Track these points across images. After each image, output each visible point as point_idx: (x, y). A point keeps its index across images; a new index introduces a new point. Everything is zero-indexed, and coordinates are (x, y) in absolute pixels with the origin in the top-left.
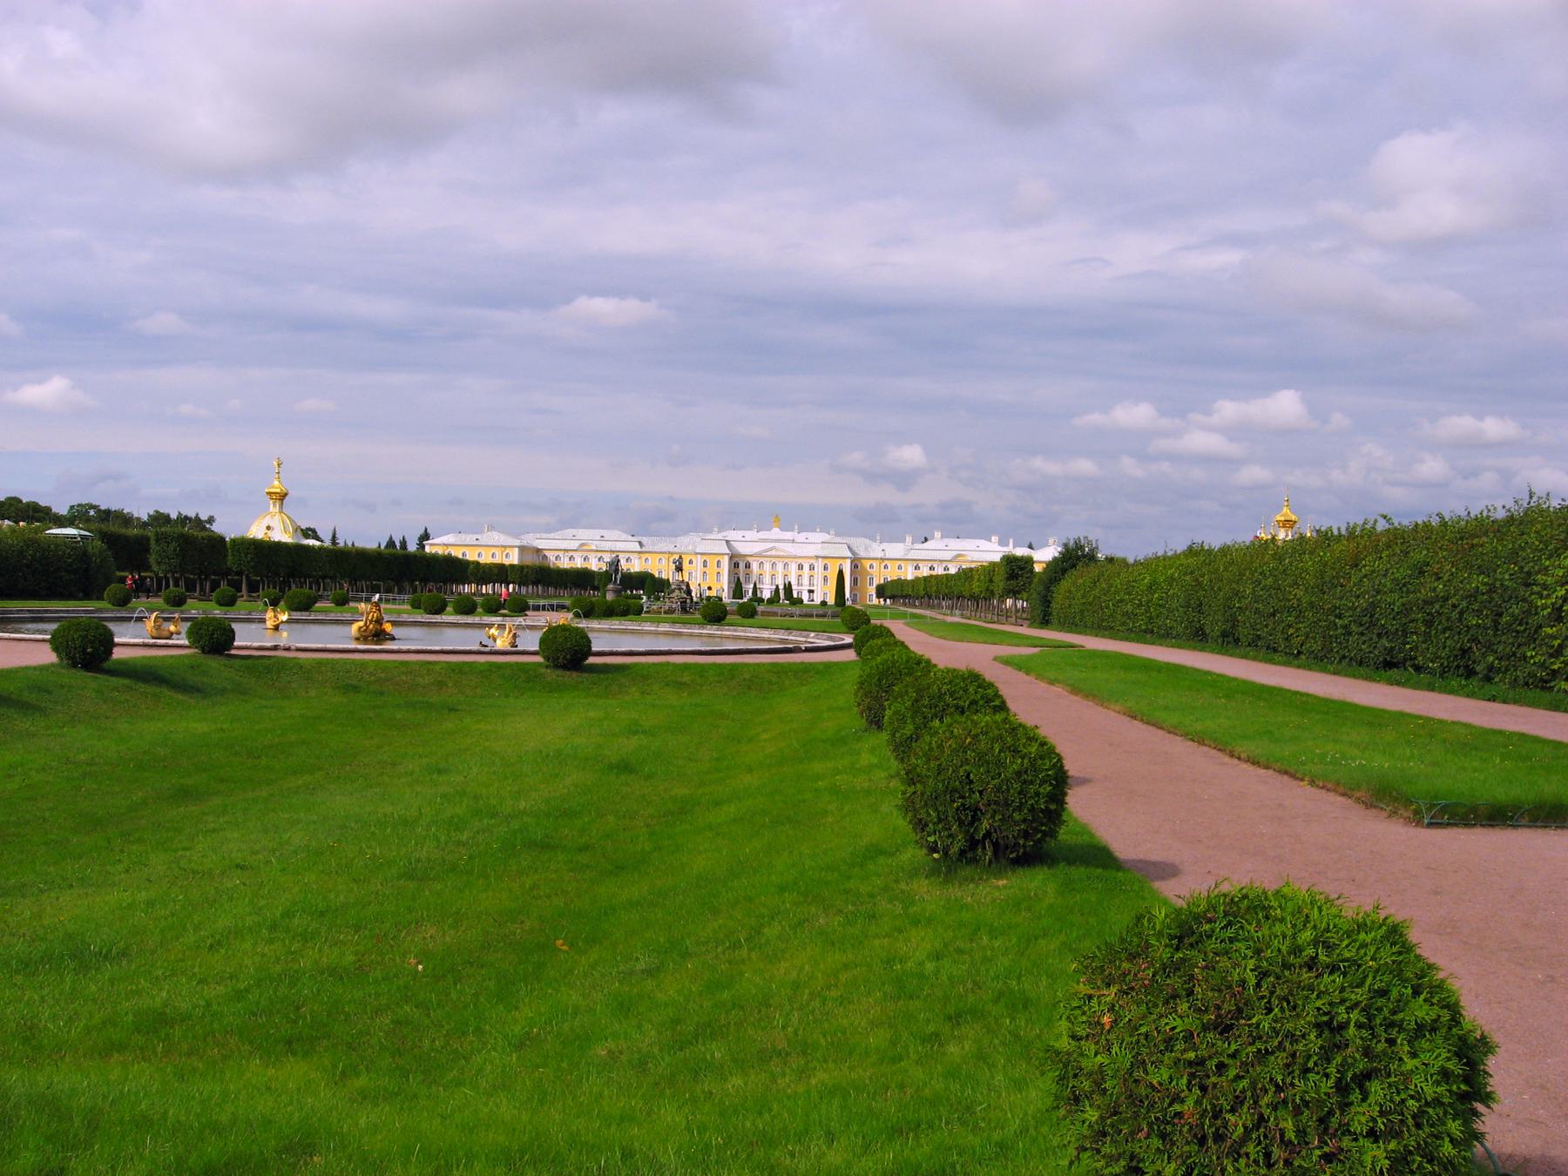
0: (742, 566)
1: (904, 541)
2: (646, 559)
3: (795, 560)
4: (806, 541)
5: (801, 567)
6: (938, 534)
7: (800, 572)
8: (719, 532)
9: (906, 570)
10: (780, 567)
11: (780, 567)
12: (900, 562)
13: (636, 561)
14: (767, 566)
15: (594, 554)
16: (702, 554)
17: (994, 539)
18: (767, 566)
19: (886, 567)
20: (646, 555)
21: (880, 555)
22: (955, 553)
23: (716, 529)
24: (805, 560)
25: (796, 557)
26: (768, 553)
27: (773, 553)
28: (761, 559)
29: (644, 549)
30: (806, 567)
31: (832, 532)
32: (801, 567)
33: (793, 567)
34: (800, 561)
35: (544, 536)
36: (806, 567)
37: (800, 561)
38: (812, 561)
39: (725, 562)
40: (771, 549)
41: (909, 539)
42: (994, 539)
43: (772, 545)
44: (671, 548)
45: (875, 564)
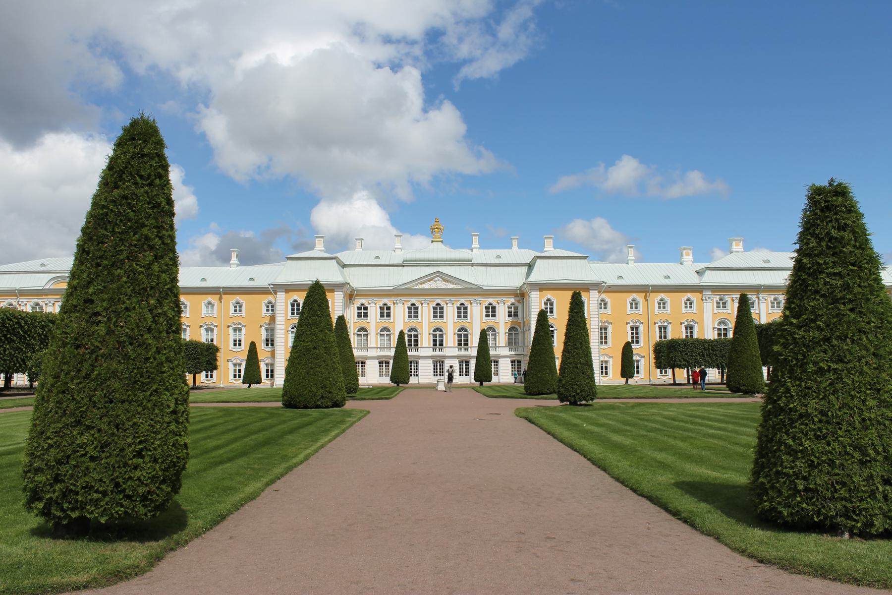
0: (374, 311)
3: (479, 298)
4: (497, 261)
9: (701, 310)
10: (450, 312)
11: (450, 312)
12: (689, 295)
14: (426, 311)
18: (426, 311)
19: (662, 304)
24: (499, 299)
26: (426, 286)
27: (440, 284)
30: (502, 312)
32: (491, 311)
40: (430, 278)
45: (639, 297)
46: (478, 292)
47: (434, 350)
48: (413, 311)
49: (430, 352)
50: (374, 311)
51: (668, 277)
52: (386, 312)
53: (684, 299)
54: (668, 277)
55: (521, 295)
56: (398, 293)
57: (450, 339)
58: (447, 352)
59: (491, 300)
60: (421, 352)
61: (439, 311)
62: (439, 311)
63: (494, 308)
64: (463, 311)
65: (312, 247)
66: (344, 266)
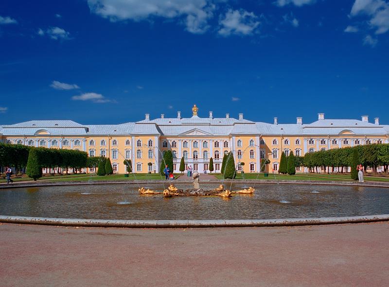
1: (295, 122)
2: (91, 142)
6: (321, 116)
7: (217, 149)
12: (297, 138)
13: (83, 143)
14: (190, 144)
17: (365, 119)
18: (190, 144)
19: (286, 142)
20: (91, 138)
21: (281, 133)
23: (147, 117)
25: (212, 136)
26: (191, 134)
28: (185, 139)
29: (88, 133)
30: (221, 144)
31: (241, 116)
33: (211, 145)
34: (216, 140)
35: (9, 126)
36: (221, 144)
37: (216, 140)
38: (227, 139)
39: (156, 141)
41: (299, 120)
42: (365, 119)
43: (195, 127)
44: (112, 133)
45: (278, 139)
47: (194, 160)
49: (192, 161)
57: (200, 156)
58: (199, 161)
63: (218, 143)
65: (144, 119)
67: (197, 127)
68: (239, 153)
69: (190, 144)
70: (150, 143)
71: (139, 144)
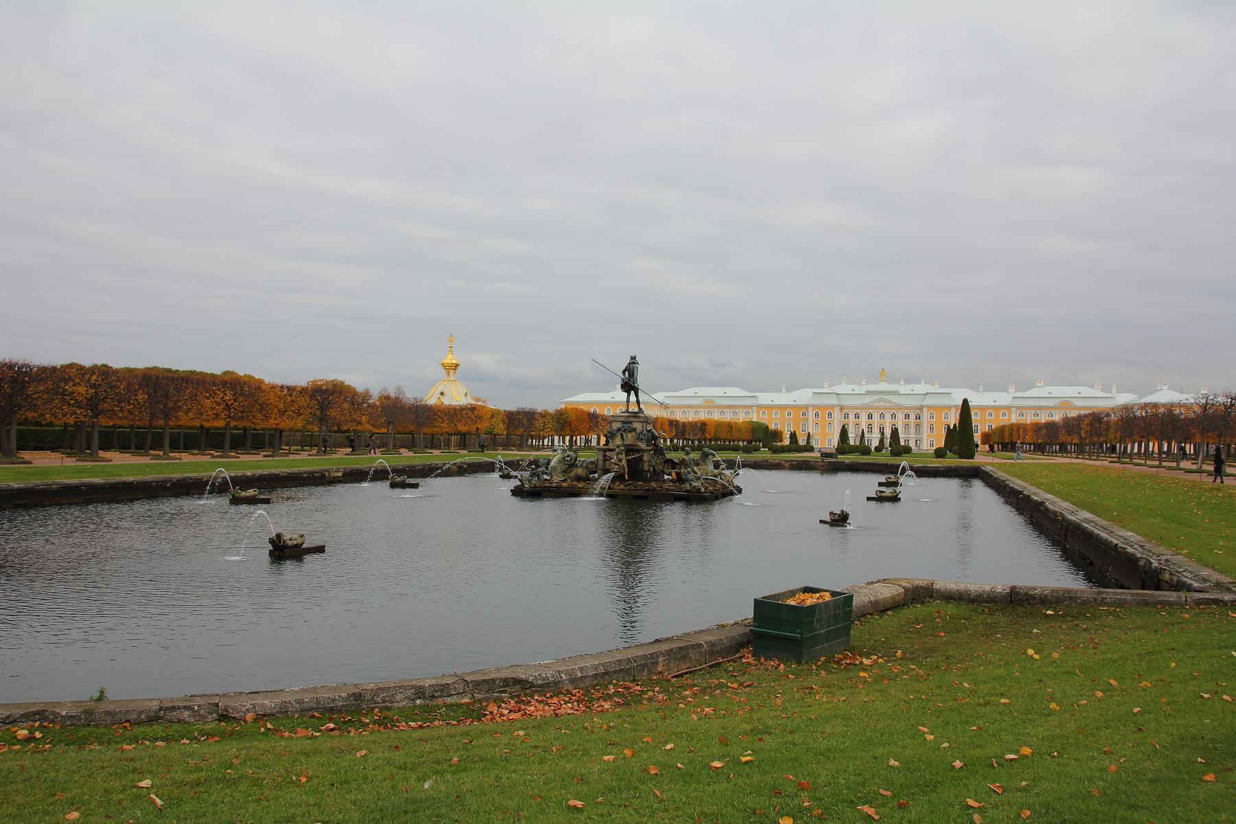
0: (851, 417)
5: (907, 416)
8: (831, 386)
10: (888, 416)
11: (888, 416)
15: (715, 410)
16: (814, 407)
19: (990, 414)
22: (1060, 400)
30: (912, 417)
46: (900, 407)
48: (870, 416)
50: (851, 417)
51: (995, 401)
52: (857, 417)
53: (1001, 413)
54: (995, 401)
55: (921, 408)
56: (863, 407)
59: (907, 411)
60: (874, 435)
61: (882, 416)
62: (882, 416)
64: (894, 416)
66: (838, 394)
67: (886, 397)
68: (932, 429)
69: (876, 414)
70: (830, 415)
71: (817, 415)
